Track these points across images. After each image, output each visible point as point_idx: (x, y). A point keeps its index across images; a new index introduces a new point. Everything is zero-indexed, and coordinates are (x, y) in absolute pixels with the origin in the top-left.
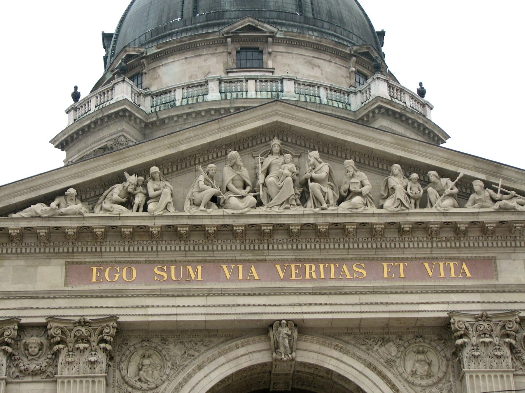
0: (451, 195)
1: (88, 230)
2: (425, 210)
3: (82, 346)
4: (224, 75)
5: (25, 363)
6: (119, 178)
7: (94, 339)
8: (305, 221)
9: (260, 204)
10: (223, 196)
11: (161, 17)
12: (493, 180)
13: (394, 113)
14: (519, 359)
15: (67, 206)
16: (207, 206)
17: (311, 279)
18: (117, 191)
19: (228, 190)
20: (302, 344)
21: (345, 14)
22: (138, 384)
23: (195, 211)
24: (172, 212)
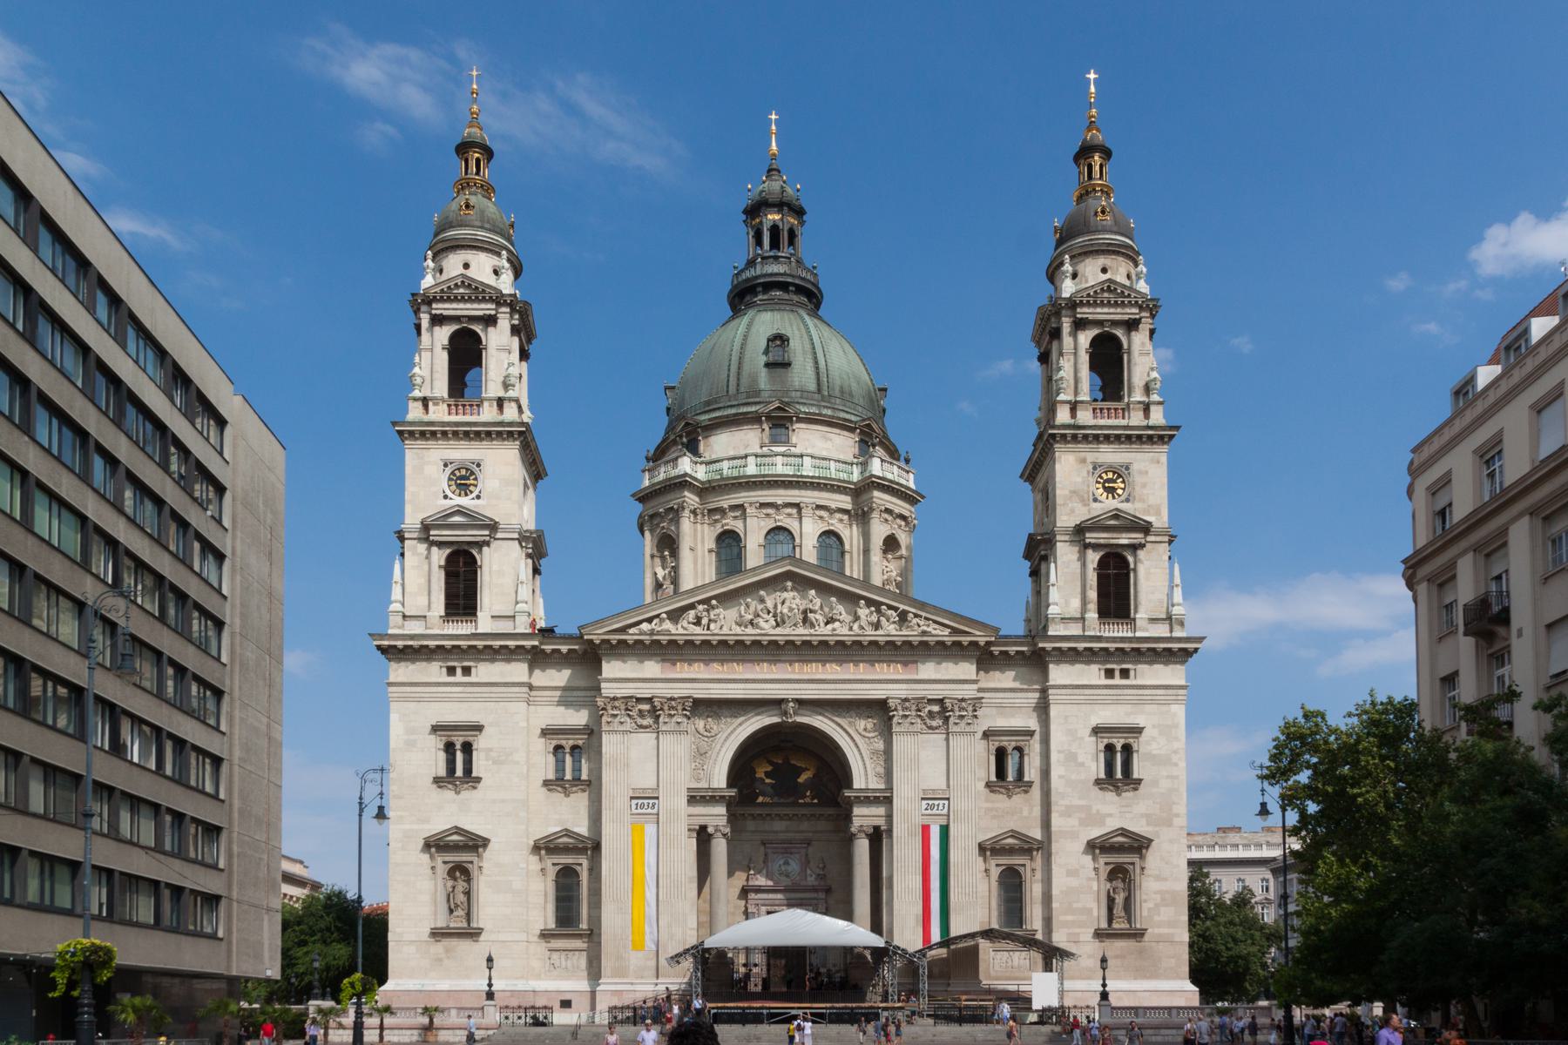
0: (894, 622)
1: (675, 642)
2: (878, 633)
3: (673, 712)
4: (759, 451)
5: (640, 721)
6: (692, 606)
7: (680, 707)
8: (805, 638)
9: (778, 625)
10: (755, 622)
11: (712, 389)
12: (919, 613)
13: (884, 485)
14: (925, 724)
15: (660, 625)
16: (746, 627)
17: (807, 673)
18: (692, 614)
19: (758, 616)
20: (801, 711)
21: (854, 385)
22: (705, 734)
23: (738, 630)
24: (725, 630)
